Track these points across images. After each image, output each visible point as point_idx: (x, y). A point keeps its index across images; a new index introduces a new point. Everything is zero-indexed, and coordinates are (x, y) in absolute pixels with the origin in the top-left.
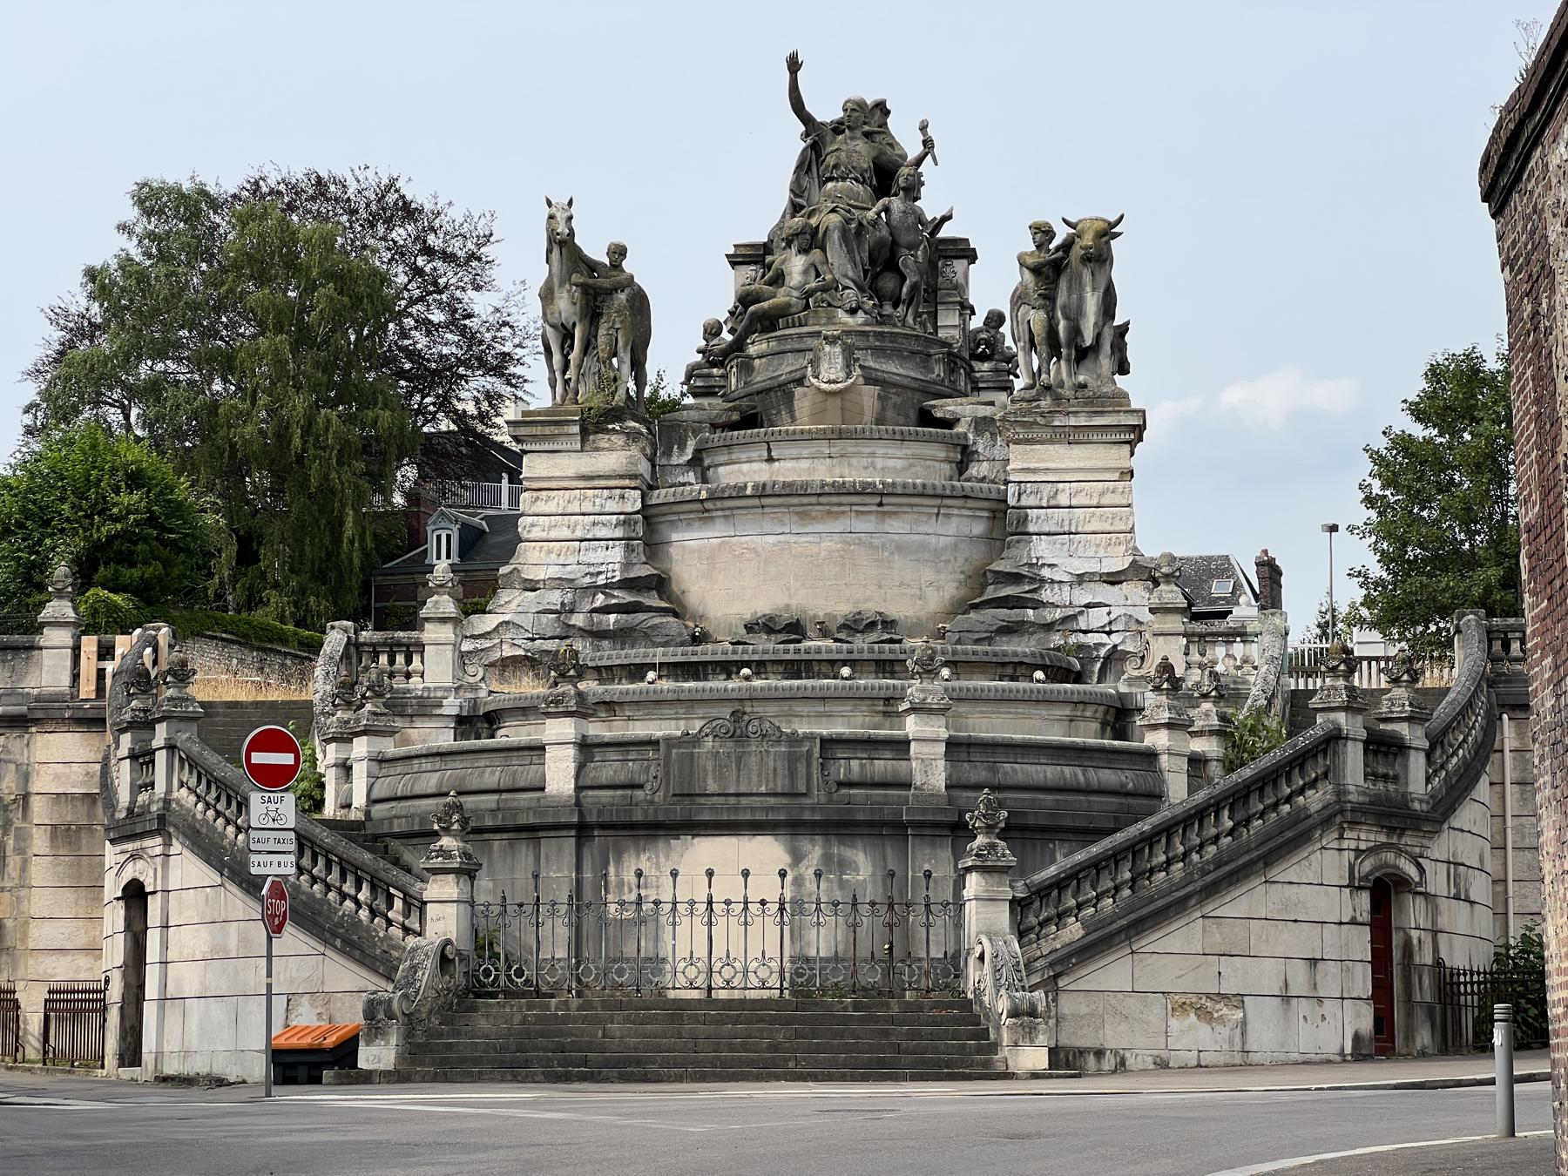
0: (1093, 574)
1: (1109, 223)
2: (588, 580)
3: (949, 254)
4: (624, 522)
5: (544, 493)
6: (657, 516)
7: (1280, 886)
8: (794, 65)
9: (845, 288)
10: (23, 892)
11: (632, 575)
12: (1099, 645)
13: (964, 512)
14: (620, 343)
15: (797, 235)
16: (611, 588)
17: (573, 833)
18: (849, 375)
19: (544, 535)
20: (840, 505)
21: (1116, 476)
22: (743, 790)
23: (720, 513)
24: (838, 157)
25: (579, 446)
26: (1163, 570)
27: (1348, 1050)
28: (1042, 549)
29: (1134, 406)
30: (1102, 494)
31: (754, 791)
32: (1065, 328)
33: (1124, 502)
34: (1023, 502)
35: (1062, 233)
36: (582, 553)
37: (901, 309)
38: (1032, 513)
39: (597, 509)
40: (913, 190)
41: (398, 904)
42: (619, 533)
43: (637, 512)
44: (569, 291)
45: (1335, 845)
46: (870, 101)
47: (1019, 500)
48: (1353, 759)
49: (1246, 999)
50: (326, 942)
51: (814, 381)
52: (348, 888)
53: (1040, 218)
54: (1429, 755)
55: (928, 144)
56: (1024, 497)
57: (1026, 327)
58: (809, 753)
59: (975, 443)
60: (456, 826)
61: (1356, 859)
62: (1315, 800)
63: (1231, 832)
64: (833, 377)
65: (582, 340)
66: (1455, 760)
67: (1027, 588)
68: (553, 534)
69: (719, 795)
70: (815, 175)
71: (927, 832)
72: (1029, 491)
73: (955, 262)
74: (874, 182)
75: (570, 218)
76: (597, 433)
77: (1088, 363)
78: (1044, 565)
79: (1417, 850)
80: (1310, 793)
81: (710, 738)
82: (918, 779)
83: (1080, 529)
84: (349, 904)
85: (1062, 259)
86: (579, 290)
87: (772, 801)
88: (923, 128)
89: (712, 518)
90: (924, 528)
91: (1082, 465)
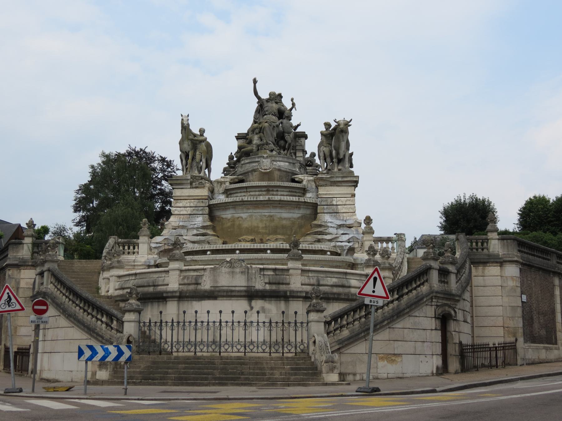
1: (348, 122)
2: (192, 226)
5: (179, 201)
7: (413, 317)
8: (255, 82)
10: (16, 318)
12: (346, 246)
13: (304, 207)
16: (199, 229)
17: (176, 299)
19: (179, 213)
21: (350, 196)
23: (231, 207)
25: (189, 187)
27: (435, 372)
29: (355, 175)
30: (346, 201)
32: (335, 153)
33: (353, 203)
35: (333, 125)
36: (190, 218)
37: (286, 152)
39: (194, 206)
40: (289, 118)
45: (430, 304)
46: (277, 93)
48: (434, 276)
49: (403, 355)
50: (91, 335)
52: (99, 317)
53: (327, 121)
54: (457, 274)
55: (293, 105)
57: (323, 152)
60: (134, 296)
61: (437, 308)
62: (424, 289)
63: (397, 299)
66: (463, 277)
67: (324, 229)
68: (182, 213)
70: (261, 114)
73: (301, 138)
74: (278, 116)
75: (188, 120)
77: (341, 164)
79: (454, 306)
80: (422, 286)
83: (339, 212)
86: (190, 141)
88: (292, 100)
89: (229, 208)
91: (340, 192)
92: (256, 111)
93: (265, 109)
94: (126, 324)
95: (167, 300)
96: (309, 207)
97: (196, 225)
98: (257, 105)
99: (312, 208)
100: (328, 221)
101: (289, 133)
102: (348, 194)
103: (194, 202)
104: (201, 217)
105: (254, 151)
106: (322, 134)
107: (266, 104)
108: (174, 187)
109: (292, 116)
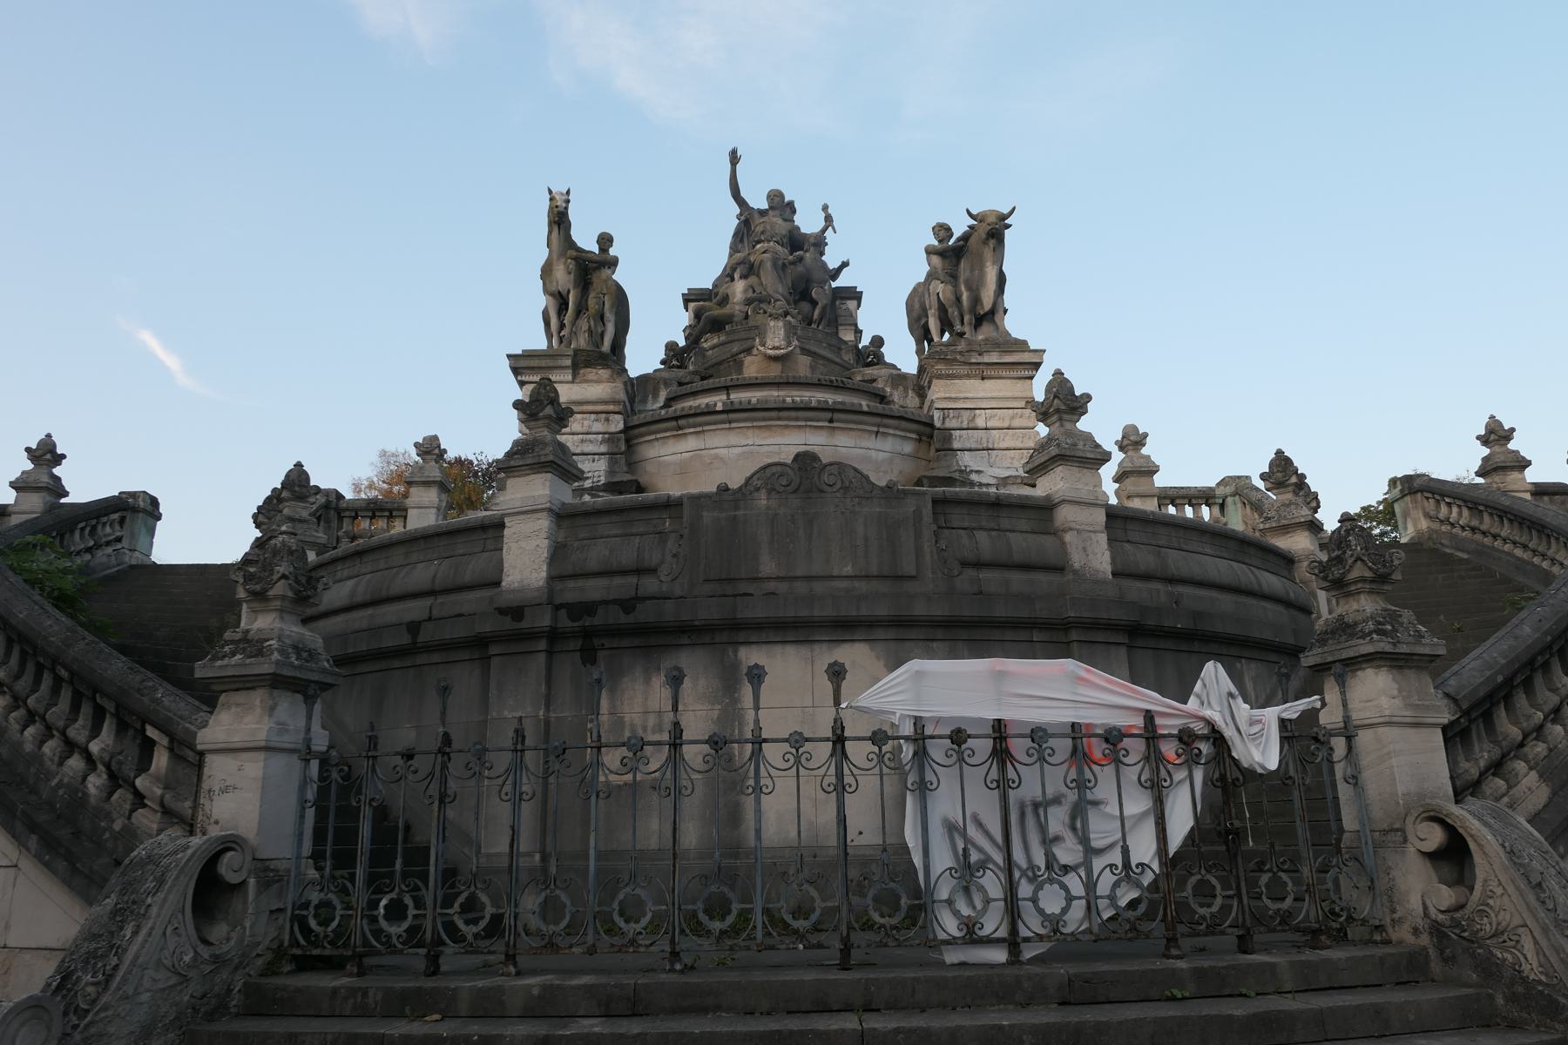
0: (1016, 477)
4: (609, 439)
8: (734, 158)
9: (776, 300)
11: (616, 480)
14: (607, 306)
15: (739, 264)
18: (789, 344)
20: (797, 419)
21: (1022, 404)
22: (817, 569)
23: (692, 430)
24: (765, 227)
26: (1132, 438)
28: (967, 460)
29: (1031, 348)
30: (1013, 418)
31: (836, 572)
32: (968, 297)
34: (948, 424)
35: (959, 229)
38: (956, 433)
39: (585, 429)
41: (161, 760)
42: (603, 449)
43: (621, 432)
44: (565, 263)
47: (943, 423)
51: (761, 348)
52: (78, 732)
56: (947, 420)
57: (936, 298)
58: (918, 514)
60: (280, 588)
64: (776, 344)
65: (574, 303)
69: (779, 579)
71: (1100, 637)
72: (951, 415)
76: (586, 367)
81: (763, 494)
82: (1077, 560)
83: (996, 446)
84: (75, 763)
86: (573, 262)
87: (863, 587)
88: (825, 208)
91: (994, 395)
92: (736, 235)
94: (218, 769)
95: (493, 650)
96: (908, 435)
97: (590, 481)
99: (916, 439)
100: (968, 470)
101: (823, 283)
103: (583, 419)
104: (602, 461)
105: (736, 319)
106: (929, 251)
107: (758, 219)
108: (524, 378)
109: (826, 244)
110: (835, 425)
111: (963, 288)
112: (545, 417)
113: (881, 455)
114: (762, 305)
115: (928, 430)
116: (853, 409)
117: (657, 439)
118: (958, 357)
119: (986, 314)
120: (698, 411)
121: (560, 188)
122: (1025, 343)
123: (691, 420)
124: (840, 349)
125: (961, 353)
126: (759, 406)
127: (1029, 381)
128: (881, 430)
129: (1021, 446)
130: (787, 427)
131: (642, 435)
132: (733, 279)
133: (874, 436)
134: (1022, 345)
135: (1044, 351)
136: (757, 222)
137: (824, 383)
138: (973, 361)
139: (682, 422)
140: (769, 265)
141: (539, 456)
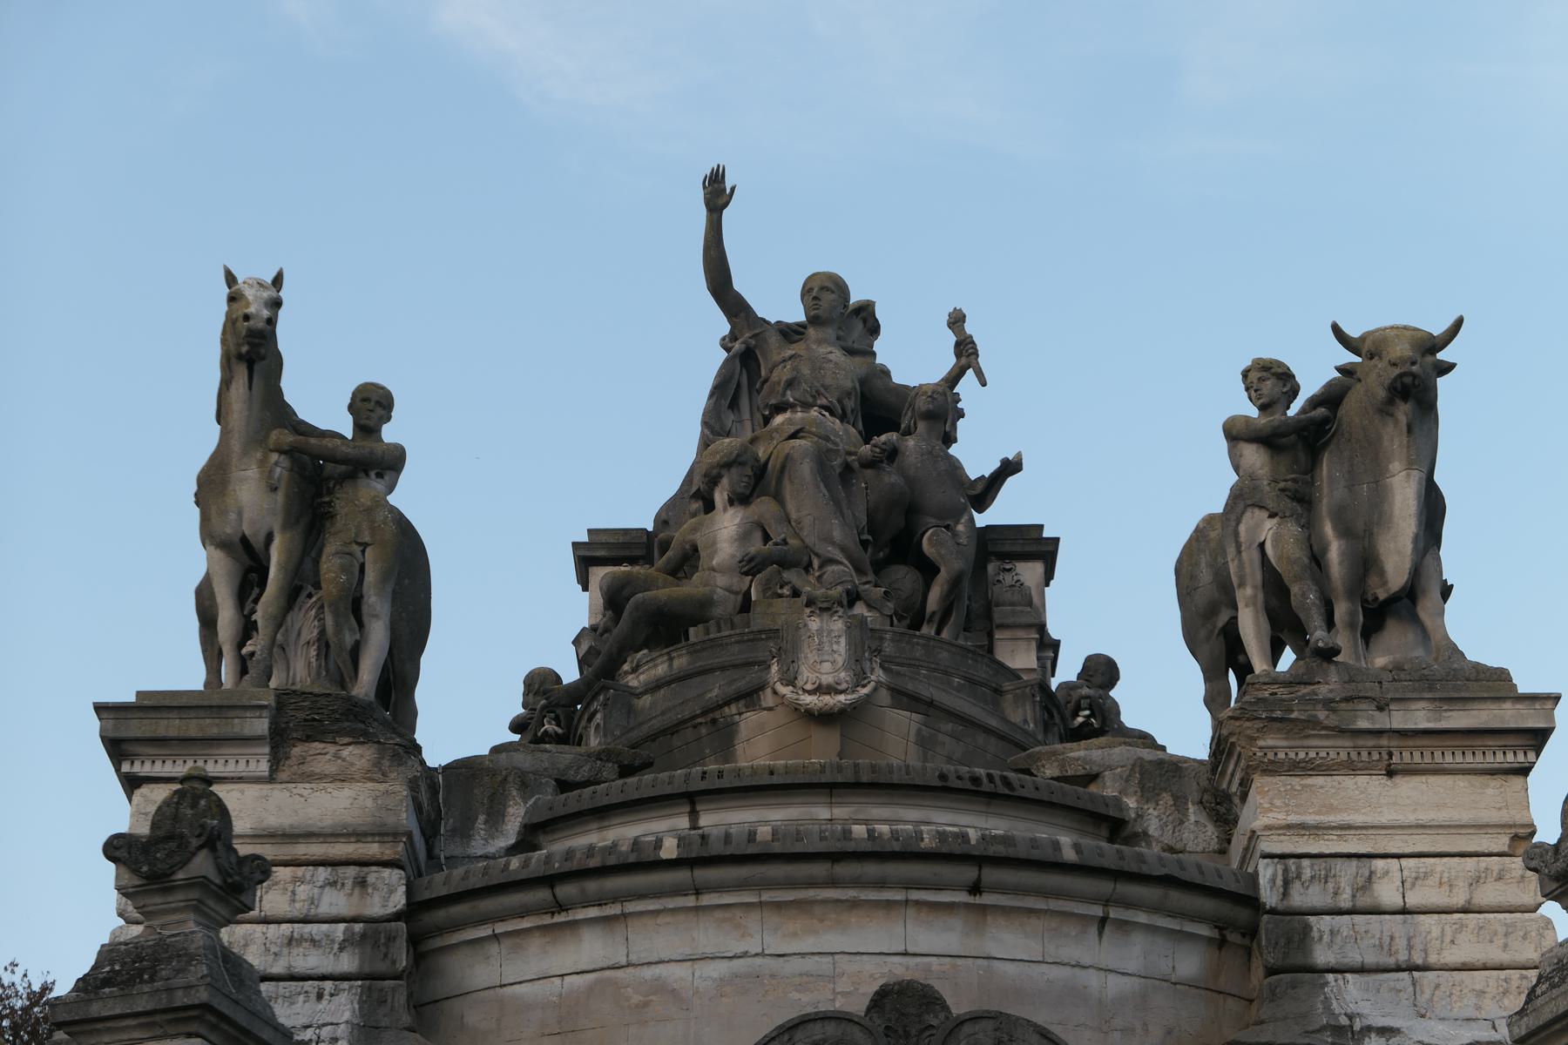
3: (1007, 548)
4: (364, 936)
6: (441, 930)
8: (717, 193)
14: (371, 576)
15: (728, 465)
18: (860, 679)
20: (881, 884)
21: (1502, 843)
23: (593, 912)
25: (263, 767)
29: (1521, 690)
30: (1476, 881)
32: (1342, 554)
35: (1313, 379)
39: (299, 909)
42: (347, 962)
43: (397, 917)
44: (262, 463)
47: (1285, 894)
51: (785, 690)
55: (966, 350)
56: (1296, 887)
57: (1256, 555)
59: (1140, 816)
64: (827, 679)
65: (282, 567)
70: (746, 415)
72: (1307, 873)
76: (309, 739)
78: (1368, 1030)
83: (1433, 959)
85: (1326, 421)
86: (285, 461)
88: (957, 321)
89: (574, 924)
90: (1071, 952)
91: (1424, 817)
92: (719, 389)
93: (775, 376)
98: (724, 355)
99: (1210, 940)
100: (1357, 1026)
101: (949, 517)
102: (1482, 827)
104: (343, 998)
105: (717, 611)
106: (1236, 433)
107: (777, 351)
108: (138, 768)
109: (961, 414)
110: (987, 899)
111: (1328, 530)
112: (191, 884)
113: (1115, 984)
114: (786, 575)
115: (1243, 914)
116: (1036, 854)
117: (496, 937)
118: (1322, 715)
119: (1394, 599)
120: (612, 861)
121: (254, 269)
122: (1502, 676)
123: (592, 886)
124: (998, 692)
125: (1328, 704)
126: (777, 848)
127: (1516, 781)
128: (1114, 913)
129: (1505, 958)
130: (854, 904)
131: (458, 926)
132: (709, 507)
133: (1094, 930)
134: (1495, 683)
135: (1556, 698)
136: (776, 358)
137: (954, 783)
138: (1363, 724)
139: (566, 891)
140: (806, 469)
141: (170, 990)
